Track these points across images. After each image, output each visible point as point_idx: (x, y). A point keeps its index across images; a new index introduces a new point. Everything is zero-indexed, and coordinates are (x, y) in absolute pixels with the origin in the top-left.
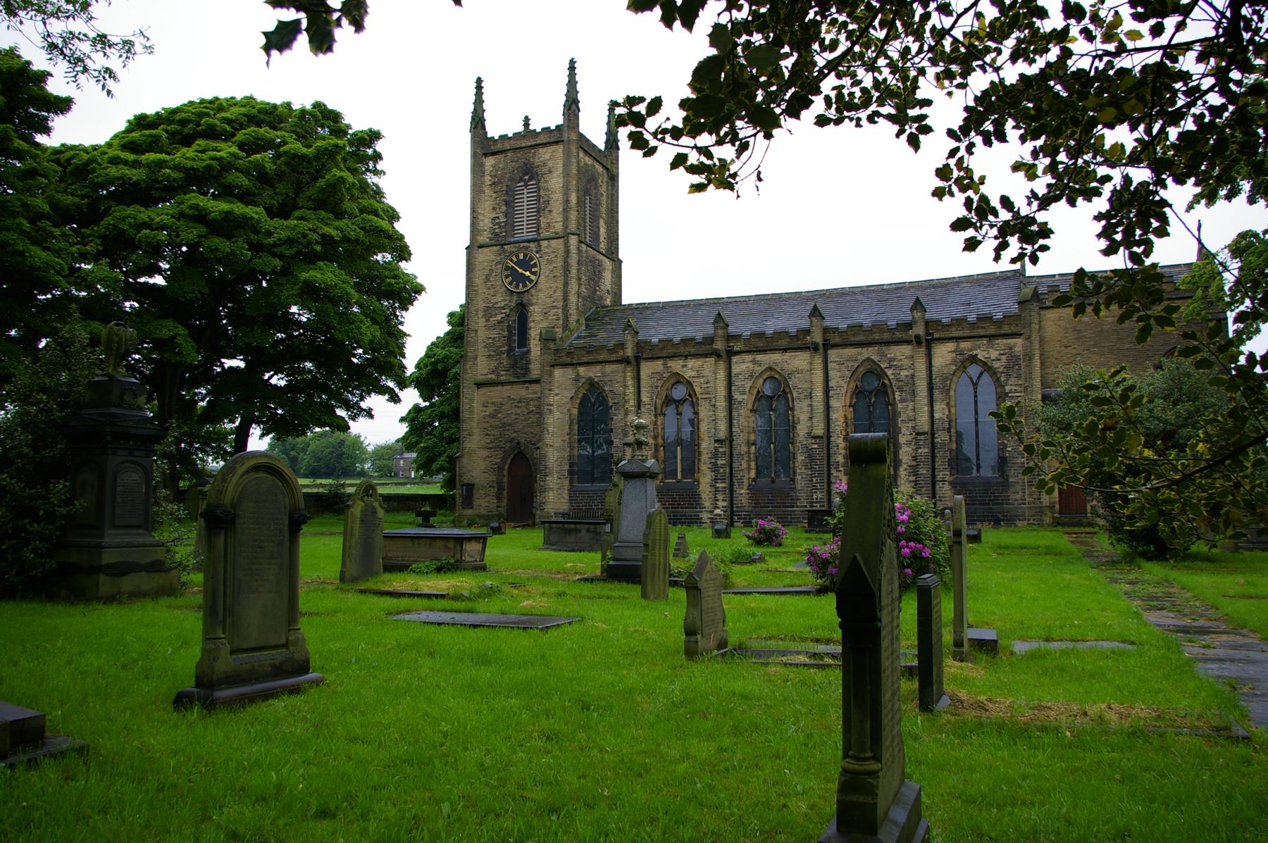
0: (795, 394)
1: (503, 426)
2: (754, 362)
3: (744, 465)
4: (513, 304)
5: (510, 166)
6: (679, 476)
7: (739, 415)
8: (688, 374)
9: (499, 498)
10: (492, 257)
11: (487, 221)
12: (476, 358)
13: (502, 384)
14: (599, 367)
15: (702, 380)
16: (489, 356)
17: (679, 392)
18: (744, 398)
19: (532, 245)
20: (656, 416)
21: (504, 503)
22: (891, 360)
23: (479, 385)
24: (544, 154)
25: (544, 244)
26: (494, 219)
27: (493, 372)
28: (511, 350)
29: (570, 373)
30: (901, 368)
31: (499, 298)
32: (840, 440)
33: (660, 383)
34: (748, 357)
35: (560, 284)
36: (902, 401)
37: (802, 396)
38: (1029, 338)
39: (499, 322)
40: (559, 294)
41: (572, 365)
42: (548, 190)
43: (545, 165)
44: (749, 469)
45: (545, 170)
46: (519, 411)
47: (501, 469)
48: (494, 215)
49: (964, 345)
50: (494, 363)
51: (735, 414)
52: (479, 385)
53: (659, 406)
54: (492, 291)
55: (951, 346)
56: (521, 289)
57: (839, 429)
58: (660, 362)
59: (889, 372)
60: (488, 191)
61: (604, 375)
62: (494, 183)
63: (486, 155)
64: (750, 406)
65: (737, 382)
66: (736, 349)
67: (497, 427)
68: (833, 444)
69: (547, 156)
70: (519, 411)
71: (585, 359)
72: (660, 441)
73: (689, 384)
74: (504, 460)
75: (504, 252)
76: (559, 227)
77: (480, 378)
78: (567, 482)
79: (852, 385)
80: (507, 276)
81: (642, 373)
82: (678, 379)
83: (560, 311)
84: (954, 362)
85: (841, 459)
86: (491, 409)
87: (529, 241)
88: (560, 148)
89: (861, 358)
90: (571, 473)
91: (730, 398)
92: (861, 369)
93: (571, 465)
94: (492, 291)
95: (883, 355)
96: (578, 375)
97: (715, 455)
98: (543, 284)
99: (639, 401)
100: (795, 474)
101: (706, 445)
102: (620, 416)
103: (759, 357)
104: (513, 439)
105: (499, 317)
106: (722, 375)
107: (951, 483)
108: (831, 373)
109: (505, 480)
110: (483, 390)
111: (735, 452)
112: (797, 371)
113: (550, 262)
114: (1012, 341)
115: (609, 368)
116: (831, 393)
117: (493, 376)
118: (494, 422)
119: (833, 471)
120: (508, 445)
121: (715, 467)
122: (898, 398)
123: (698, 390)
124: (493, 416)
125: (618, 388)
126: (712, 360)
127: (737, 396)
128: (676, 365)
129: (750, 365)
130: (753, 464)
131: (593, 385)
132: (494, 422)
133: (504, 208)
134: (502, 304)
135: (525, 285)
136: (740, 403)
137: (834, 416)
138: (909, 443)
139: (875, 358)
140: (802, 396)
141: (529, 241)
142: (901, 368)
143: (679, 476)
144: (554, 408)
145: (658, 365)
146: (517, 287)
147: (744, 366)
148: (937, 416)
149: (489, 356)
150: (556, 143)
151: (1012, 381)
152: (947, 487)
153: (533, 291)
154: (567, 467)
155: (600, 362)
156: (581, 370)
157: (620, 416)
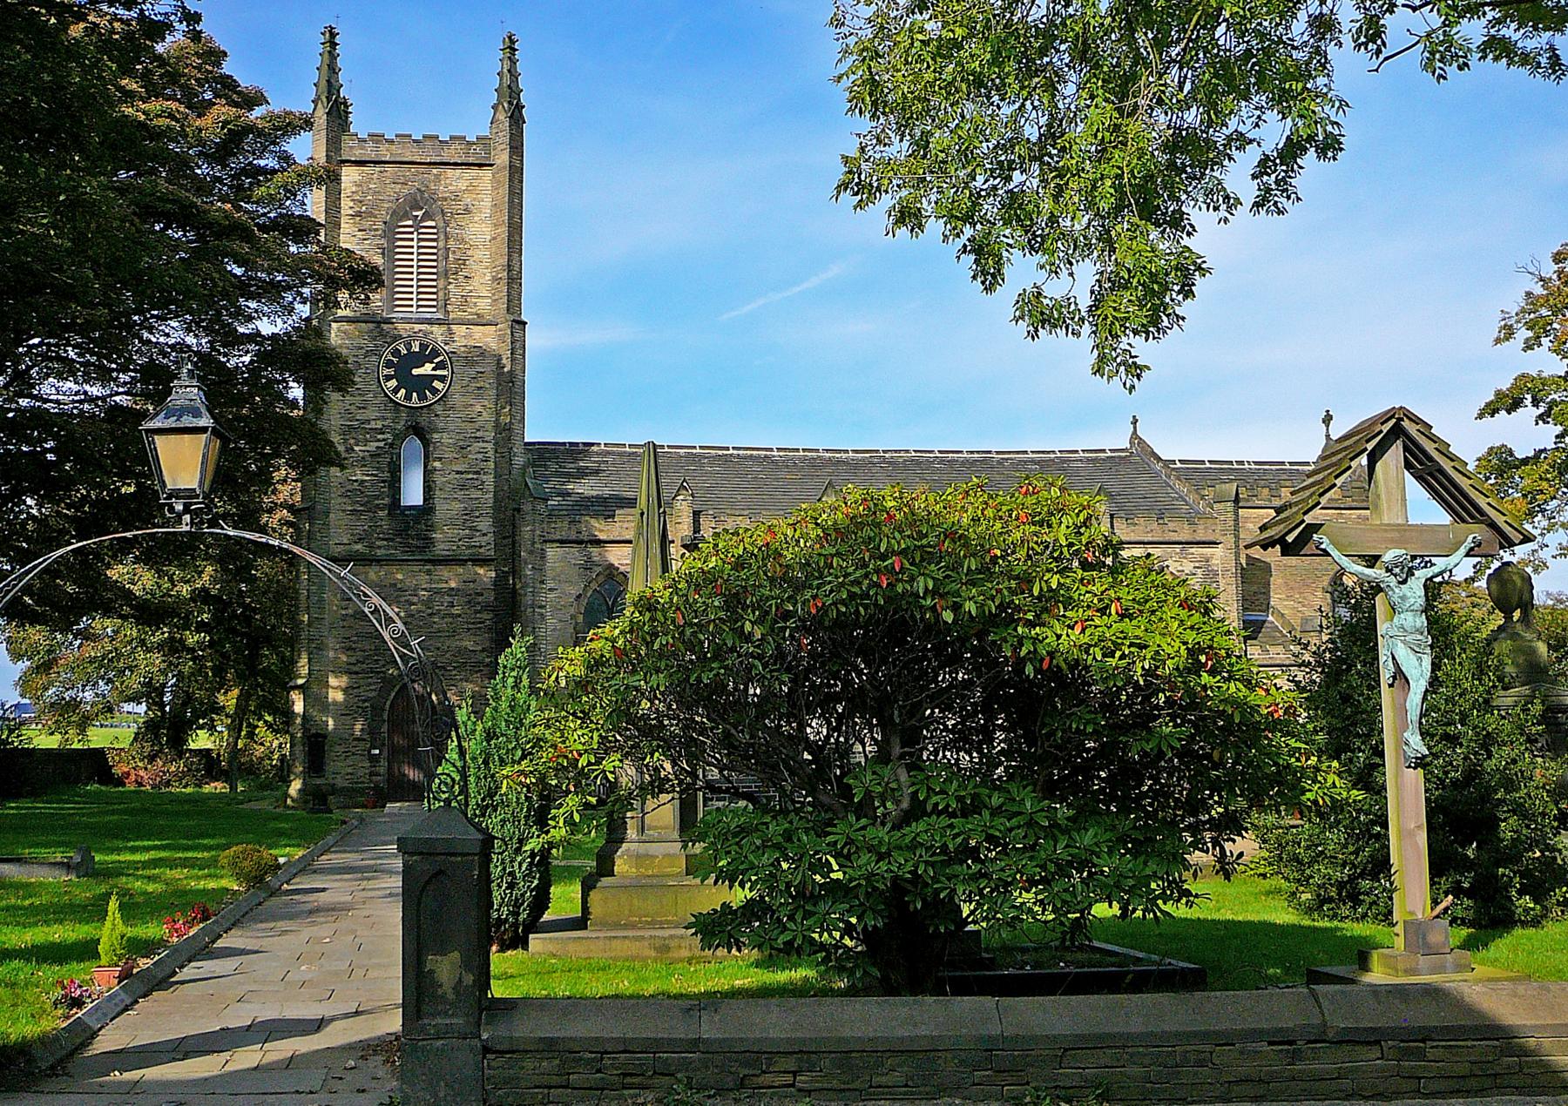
5: (392, 190)
12: (327, 514)
19: (435, 328)
24: (457, 180)
31: (371, 413)
42: (463, 241)
43: (457, 198)
50: (363, 525)
69: (463, 185)
80: (388, 378)
87: (430, 322)
105: (372, 446)
114: (1207, 551)
135: (422, 397)
141: (430, 322)
144: (548, 612)
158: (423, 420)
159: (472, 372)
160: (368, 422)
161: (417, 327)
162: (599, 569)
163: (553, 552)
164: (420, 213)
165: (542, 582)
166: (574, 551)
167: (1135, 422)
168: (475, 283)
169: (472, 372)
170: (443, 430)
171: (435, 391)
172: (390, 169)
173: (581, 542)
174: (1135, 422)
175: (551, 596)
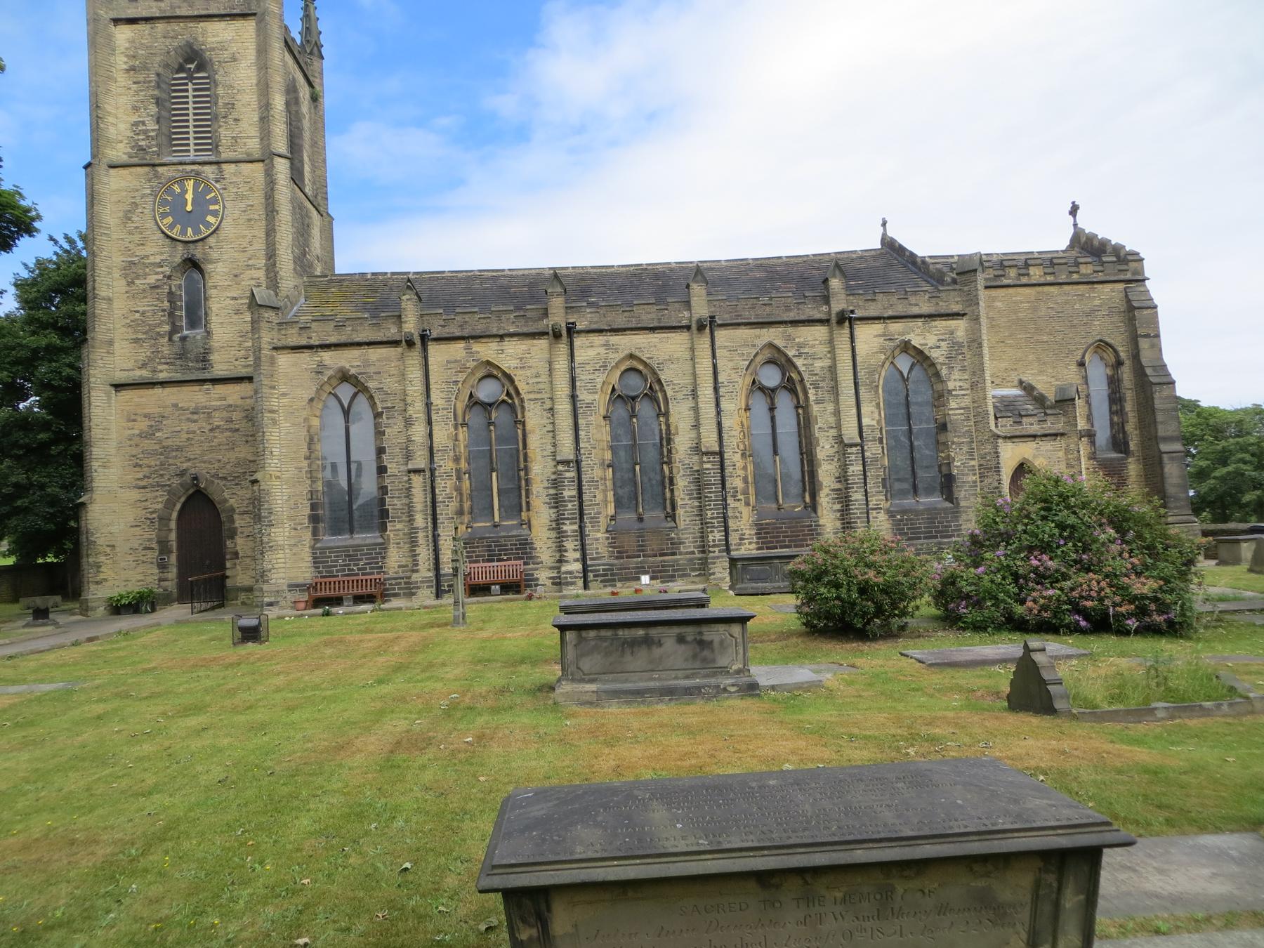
0: (669, 393)
1: (166, 451)
2: (606, 345)
3: (600, 497)
4: (178, 260)
5: (161, 45)
6: (497, 519)
7: (588, 425)
8: (507, 364)
9: (162, 566)
10: (135, 184)
11: (122, 126)
13: (163, 384)
14: (355, 353)
15: (529, 373)
16: (136, 341)
17: (488, 391)
18: (595, 398)
19: (207, 169)
20: (456, 429)
21: (173, 573)
22: (800, 346)
23: (118, 387)
25: (229, 169)
26: (136, 124)
27: (143, 366)
28: (175, 329)
29: (307, 360)
30: (814, 357)
31: (150, 249)
32: (737, 457)
33: (461, 377)
34: (598, 340)
35: (261, 234)
36: (818, 402)
37: (680, 396)
38: (977, 319)
39: (154, 287)
40: (259, 246)
41: (310, 347)
44: (606, 502)
45: (226, 55)
46: (194, 427)
47: (164, 520)
48: (135, 118)
49: (895, 327)
50: (145, 352)
51: (580, 421)
52: (118, 387)
53: (460, 412)
54: (137, 238)
55: (877, 328)
56: (190, 235)
57: (735, 441)
58: (461, 345)
59: (799, 362)
60: (122, 80)
61: (367, 363)
62: (132, 69)
63: (117, 21)
64: (603, 412)
65: (583, 377)
66: (579, 327)
67: (154, 453)
68: (727, 463)
70: (194, 427)
71: (333, 339)
72: (463, 465)
73: (510, 378)
74: (169, 505)
75: (157, 176)
76: (253, 145)
77: (121, 377)
78: (307, 535)
79: (749, 380)
80: (164, 216)
81: (431, 361)
82: (491, 372)
83: (261, 274)
84: (882, 350)
85: (738, 483)
86: (143, 425)
88: (249, 26)
89: (761, 343)
90: (314, 519)
91: (573, 397)
92: (760, 359)
93: (313, 507)
94: (137, 238)
95: (789, 339)
96: (320, 364)
97: (556, 483)
98: (228, 230)
99: (428, 405)
100: (674, 508)
101: (540, 470)
102: (396, 429)
103: (615, 339)
104: (182, 474)
105: (152, 279)
106: (562, 364)
107: (888, 512)
108: (720, 364)
109: (173, 536)
110: (127, 395)
111: (585, 479)
112: (671, 360)
113: (240, 197)
114: (952, 323)
115: (374, 354)
116: (722, 391)
117: (145, 374)
118: (148, 444)
119: (730, 500)
120: (176, 482)
121: (557, 502)
122: (812, 397)
123: (522, 387)
124: (148, 435)
125: (391, 384)
126: (543, 343)
127: (583, 396)
128: (487, 350)
129: (602, 351)
130: (610, 495)
131: (344, 377)
132: (148, 444)
133: (153, 109)
134: (158, 259)
136: (588, 406)
137: (726, 423)
138: (830, 459)
139: (780, 343)
140: (680, 396)
142: (814, 357)
143: (497, 519)
145: (457, 349)
146: (184, 232)
147: (592, 353)
148: (865, 421)
149: (136, 341)
150: (244, 16)
151: (956, 375)
152: (882, 516)
153: (212, 241)
154: (307, 511)
155: (359, 344)
156: (326, 356)
157: (396, 429)
158: (198, 252)
159: (242, 205)
160: (147, 257)
161: (189, 168)
162: (330, 373)
163: (284, 360)
164: (192, 66)
165: (273, 388)
166: (306, 359)
167: (884, 224)
168: (244, 125)
169: (242, 205)
170: (217, 261)
171: (208, 225)
172: (160, 26)
173: (310, 347)
174: (884, 224)
175: (284, 400)
